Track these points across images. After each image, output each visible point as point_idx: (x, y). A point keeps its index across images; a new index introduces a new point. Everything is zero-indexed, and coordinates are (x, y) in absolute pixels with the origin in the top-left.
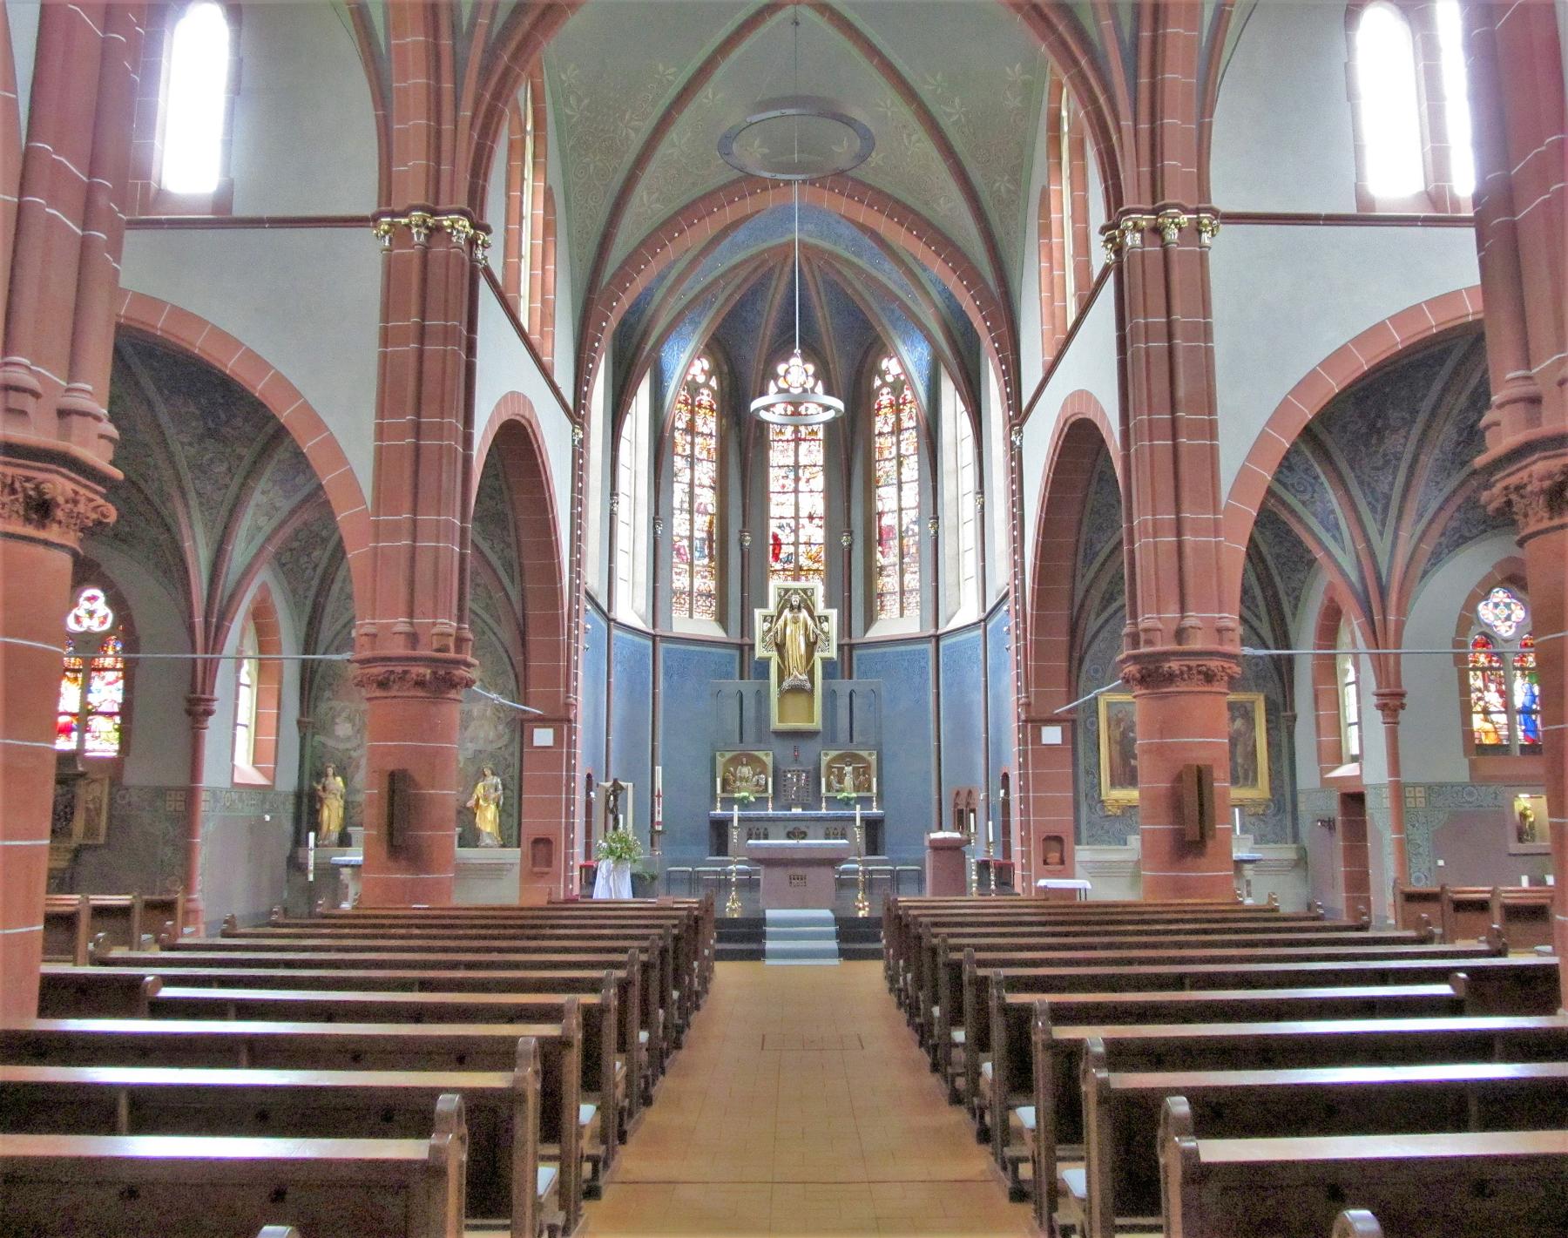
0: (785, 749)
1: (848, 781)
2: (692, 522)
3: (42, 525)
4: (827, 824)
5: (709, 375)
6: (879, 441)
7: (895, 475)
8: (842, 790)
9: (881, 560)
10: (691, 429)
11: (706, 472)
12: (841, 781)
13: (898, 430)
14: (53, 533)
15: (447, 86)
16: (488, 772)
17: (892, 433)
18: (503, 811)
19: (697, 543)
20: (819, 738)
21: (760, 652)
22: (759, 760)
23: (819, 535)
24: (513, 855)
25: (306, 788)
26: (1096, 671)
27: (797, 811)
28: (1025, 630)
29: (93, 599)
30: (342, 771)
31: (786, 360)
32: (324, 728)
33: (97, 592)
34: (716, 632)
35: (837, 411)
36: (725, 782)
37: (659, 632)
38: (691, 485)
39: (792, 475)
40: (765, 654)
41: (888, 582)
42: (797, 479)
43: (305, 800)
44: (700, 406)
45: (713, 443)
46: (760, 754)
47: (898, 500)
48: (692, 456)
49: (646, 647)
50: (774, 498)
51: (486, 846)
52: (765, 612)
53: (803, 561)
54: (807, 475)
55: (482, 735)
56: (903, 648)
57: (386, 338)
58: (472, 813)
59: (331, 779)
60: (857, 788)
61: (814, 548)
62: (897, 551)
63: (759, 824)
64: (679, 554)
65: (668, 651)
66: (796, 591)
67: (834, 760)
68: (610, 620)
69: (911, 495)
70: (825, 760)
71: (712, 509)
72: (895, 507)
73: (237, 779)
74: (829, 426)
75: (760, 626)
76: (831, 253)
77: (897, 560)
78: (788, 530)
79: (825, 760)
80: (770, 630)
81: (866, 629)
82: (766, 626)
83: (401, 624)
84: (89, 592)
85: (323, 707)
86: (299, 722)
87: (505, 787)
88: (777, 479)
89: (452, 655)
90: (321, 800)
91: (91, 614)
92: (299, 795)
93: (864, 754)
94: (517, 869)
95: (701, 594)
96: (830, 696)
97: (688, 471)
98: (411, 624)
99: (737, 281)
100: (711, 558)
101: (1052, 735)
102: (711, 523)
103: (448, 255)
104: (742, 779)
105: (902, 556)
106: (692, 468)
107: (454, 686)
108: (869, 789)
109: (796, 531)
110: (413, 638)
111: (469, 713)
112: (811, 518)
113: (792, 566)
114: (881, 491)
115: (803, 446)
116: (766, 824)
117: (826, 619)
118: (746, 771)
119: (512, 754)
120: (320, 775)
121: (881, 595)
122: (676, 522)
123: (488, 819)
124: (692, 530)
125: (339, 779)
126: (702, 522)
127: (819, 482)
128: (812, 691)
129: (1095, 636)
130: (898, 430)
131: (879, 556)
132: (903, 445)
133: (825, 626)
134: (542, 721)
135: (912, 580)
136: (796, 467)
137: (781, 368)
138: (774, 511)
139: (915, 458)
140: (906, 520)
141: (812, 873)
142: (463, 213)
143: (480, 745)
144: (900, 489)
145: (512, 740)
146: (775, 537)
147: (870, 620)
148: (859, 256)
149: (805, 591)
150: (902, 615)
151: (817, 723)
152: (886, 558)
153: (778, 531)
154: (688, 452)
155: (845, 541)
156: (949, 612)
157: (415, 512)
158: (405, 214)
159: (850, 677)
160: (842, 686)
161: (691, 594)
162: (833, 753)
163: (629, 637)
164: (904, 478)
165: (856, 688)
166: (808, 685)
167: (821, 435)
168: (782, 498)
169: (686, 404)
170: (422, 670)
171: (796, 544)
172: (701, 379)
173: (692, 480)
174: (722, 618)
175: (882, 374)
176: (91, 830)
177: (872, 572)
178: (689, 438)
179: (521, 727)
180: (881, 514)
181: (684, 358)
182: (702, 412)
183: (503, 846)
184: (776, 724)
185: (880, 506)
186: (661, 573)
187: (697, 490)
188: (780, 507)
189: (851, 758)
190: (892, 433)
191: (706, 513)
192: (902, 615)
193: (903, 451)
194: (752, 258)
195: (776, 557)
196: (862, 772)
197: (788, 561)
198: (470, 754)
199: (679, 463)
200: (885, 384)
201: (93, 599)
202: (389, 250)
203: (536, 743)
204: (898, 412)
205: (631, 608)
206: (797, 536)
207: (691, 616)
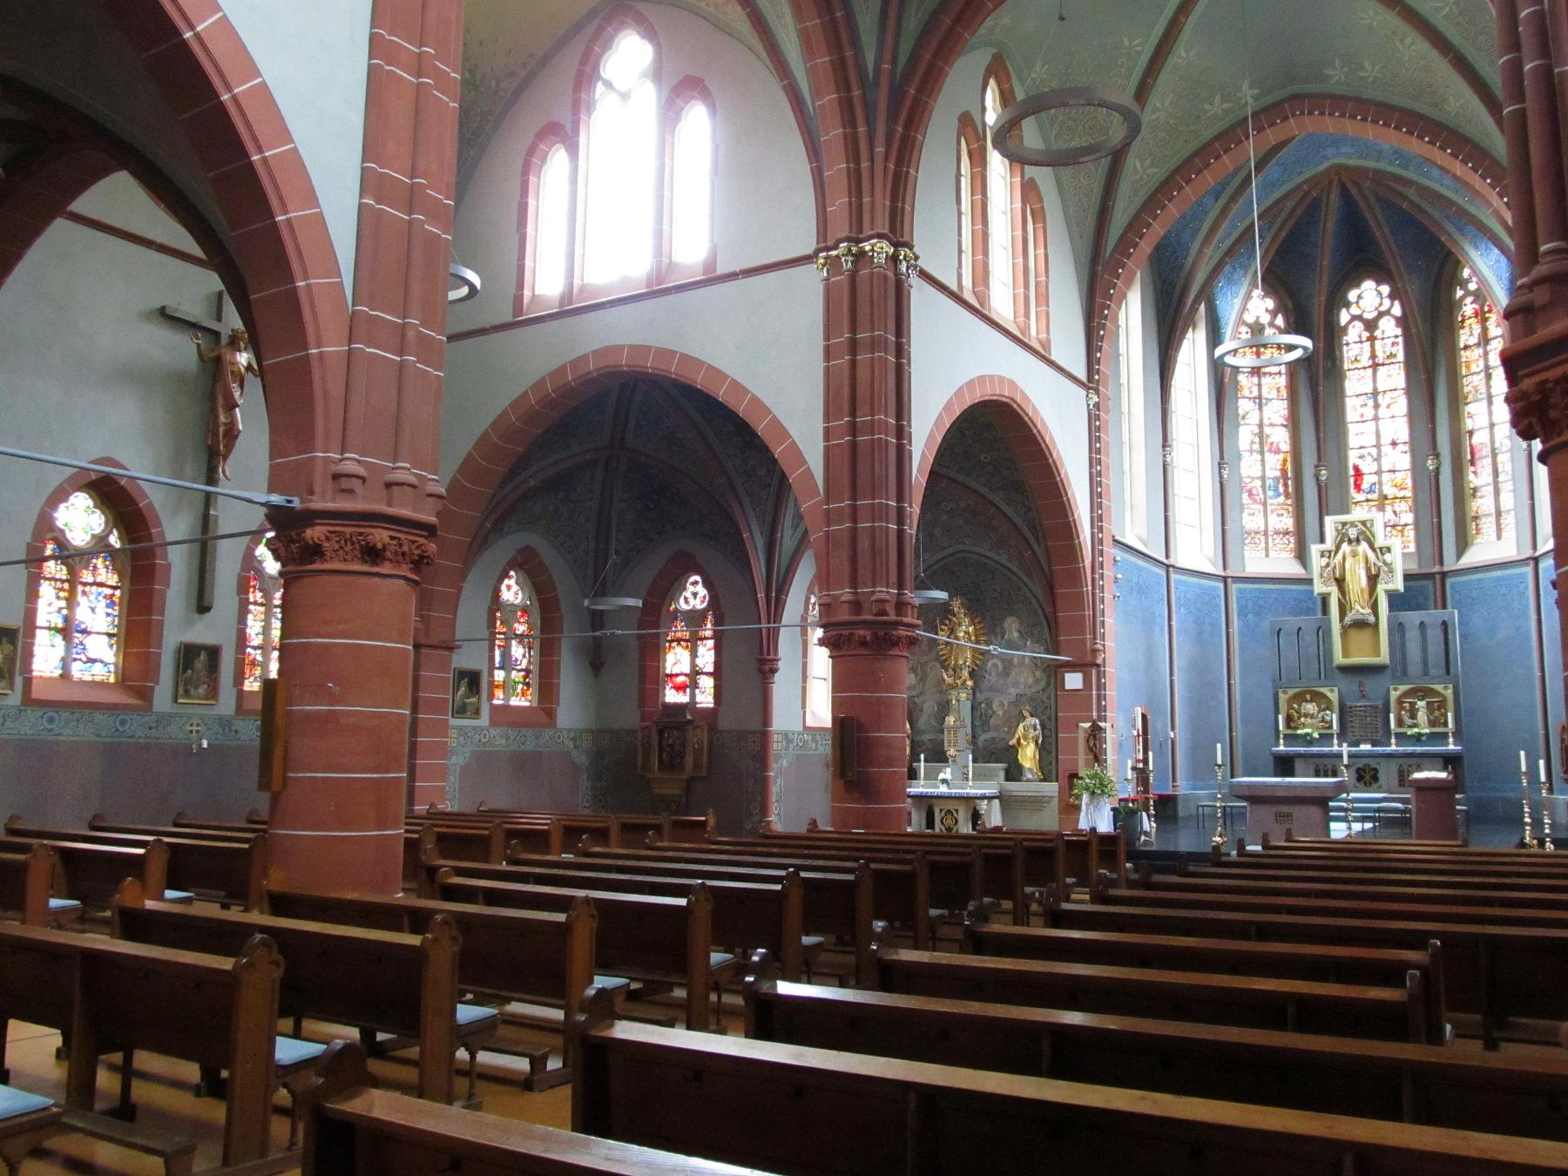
0: (1351, 684)
1: (1422, 716)
2: (1263, 461)
3: (375, 564)
4: (1401, 761)
5: (1274, 314)
7: (1483, 389)
8: (1415, 726)
9: (1473, 480)
11: (1278, 410)
12: (1413, 716)
14: (386, 569)
15: (861, 129)
16: (1026, 714)
17: (1478, 345)
18: (1042, 749)
19: (1268, 482)
20: (1389, 671)
21: (1319, 588)
22: (1323, 696)
24: (1051, 788)
29: (695, 583)
31: (1358, 286)
33: (698, 578)
35: (1305, 348)
36: (1289, 719)
37: (1229, 573)
38: (1261, 426)
39: (1371, 403)
40: (1324, 590)
41: (1483, 504)
42: (1377, 406)
45: (1282, 381)
48: (1260, 397)
50: (1353, 429)
53: (1389, 491)
56: (1499, 573)
57: (828, 354)
58: (1014, 750)
60: (1432, 723)
61: (1399, 477)
62: (1489, 469)
63: (1327, 761)
64: (1250, 494)
65: (1241, 591)
67: (1406, 694)
70: (1394, 695)
71: (1285, 447)
72: (1486, 424)
73: (809, 723)
74: (1292, 367)
75: (1317, 562)
76: (1376, 171)
77: (1490, 479)
78: (1369, 459)
79: (1394, 695)
82: (1324, 561)
83: (845, 594)
84: (692, 579)
87: (1043, 727)
88: (1354, 408)
89: (893, 617)
91: (695, 595)
93: (1439, 688)
94: (1055, 801)
95: (1277, 533)
96: (1397, 629)
98: (856, 594)
99: (1283, 216)
100: (1287, 496)
102: (1285, 461)
103: (872, 274)
104: (1306, 716)
105: (1496, 473)
106: (1260, 408)
107: (896, 643)
108: (1446, 724)
109: (1378, 459)
110: (856, 606)
113: (1375, 496)
114: (1470, 408)
115: (1381, 370)
117: (1389, 550)
118: (1310, 708)
121: (1476, 518)
123: (1028, 756)
124: (1263, 470)
127: (1401, 405)
128: (1376, 626)
130: (1485, 340)
131: (1471, 477)
133: (1388, 557)
136: (1375, 393)
138: (1353, 441)
142: (880, 236)
143: (1021, 689)
145: (1048, 684)
146: (1356, 468)
147: (1463, 545)
148: (1406, 168)
149: (1364, 523)
150: (1499, 537)
151: (1384, 657)
152: (1480, 477)
153: (1359, 462)
155: (1430, 464)
157: (854, 497)
158: (836, 247)
159: (1444, 607)
160: (1412, 618)
161: (1266, 534)
162: (1403, 688)
163: (1195, 580)
165: (1426, 620)
166: (1372, 619)
167: (1401, 357)
170: (861, 632)
171: (1379, 473)
172: (1265, 319)
173: (1261, 420)
176: (697, 766)
178: (1255, 380)
179: (1055, 673)
180: (1471, 433)
183: (1045, 780)
184: (1339, 658)
185: (1469, 424)
187: (1267, 430)
188: (1359, 436)
189: (1424, 693)
190: (1478, 345)
191: (1278, 451)
192: (1499, 537)
194: (1299, 187)
195: (1358, 487)
197: (1371, 491)
198: (1012, 698)
199: (1244, 406)
200: (1468, 293)
201: (695, 583)
202: (827, 279)
203: (1068, 687)
204: (1484, 321)
206: (1380, 465)
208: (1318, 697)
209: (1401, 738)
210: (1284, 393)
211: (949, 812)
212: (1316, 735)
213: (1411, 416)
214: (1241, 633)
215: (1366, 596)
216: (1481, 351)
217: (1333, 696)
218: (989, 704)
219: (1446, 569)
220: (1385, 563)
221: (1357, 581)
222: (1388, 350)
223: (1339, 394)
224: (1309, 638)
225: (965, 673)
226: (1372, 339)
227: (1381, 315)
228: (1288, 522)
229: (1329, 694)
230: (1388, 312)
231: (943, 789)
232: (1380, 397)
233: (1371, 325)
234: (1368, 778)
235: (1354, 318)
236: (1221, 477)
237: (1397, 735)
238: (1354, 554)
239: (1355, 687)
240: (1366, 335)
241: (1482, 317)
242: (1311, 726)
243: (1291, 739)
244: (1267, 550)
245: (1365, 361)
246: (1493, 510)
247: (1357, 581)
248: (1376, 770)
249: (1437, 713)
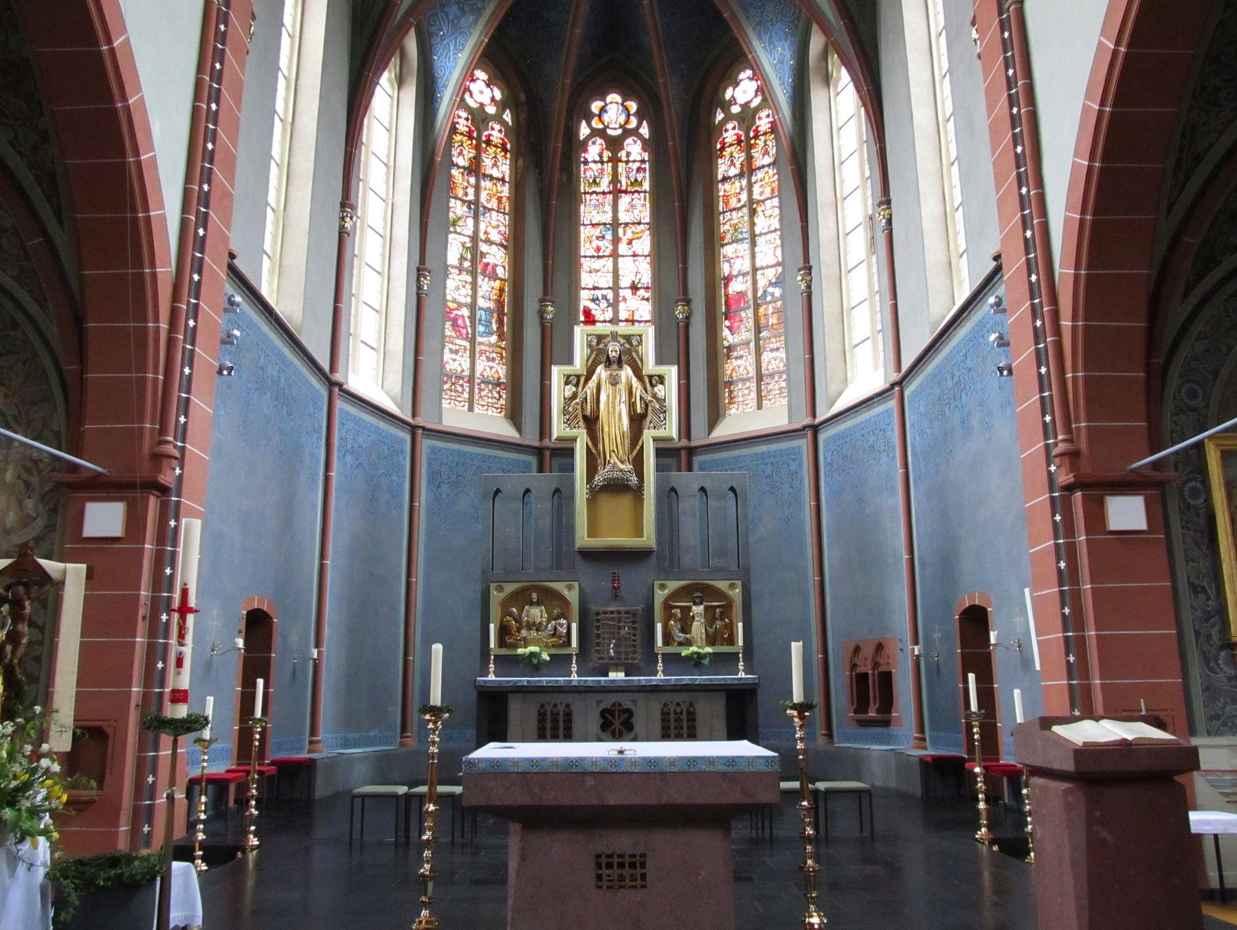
0: (598, 580)
1: (698, 628)
5: (502, 106)
6: (723, 189)
7: (745, 228)
8: (688, 643)
9: (728, 337)
10: (474, 168)
11: (496, 225)
12: (686, 629)
13: (748, 170)
19: (480, 314)
20: (653, 560)
21: (558, 428)
23: (644, 310)
26: (1192, 395)
27: (617, 676)
28: (1056, 315)
34: (506, 431)
36: (504, 631)
37: (420, 421)
38: (475, 238)
39: (609, 236)
40: (568, 432)
41: (740, 366)
42: (616, 241)
44: (488, 142)
45: (505, 191)
46: (559, 587)
47: (751, 255)
49: (403, 441)
50: (586, 264)
52: (568, 369)
54: (629, 235)
56: (763, 448)
60: (711, 640)
62: (751, 324)
63: (558, 699)
64: (455, 326)
65: (434, 450)
66: (614, 336)
67: (675, 595)
68: (334, 387)
69: (769, 252)
70: (660, 595)
72: (747, 266)
75: (558, 392)
77: (751, 336)
78: (604, 304)
79: (660, 595)
80: (574, 396)
81: (709, 433)
88: (589, 240)
93: (722, 585)
96: (668, 495)
97: (470, 221)
100: (501, 338)
101: (1126, 513)
102: (501, 290)
104: (530, 626)
105: (758, 329)
106: (476, 218)
108: (731, 641)
109: (614, 305)
112: (634, 288)
114: (728, 250)
115: (624, 200)
116: (568, 698)
117: (661, 379)
118: (536, 613)
121: (730, 383)
122: (450, 284)
126: (487, 287)
127: (644, 244)
128: (638, 492)
129: (1184, 329)
130: (748, 170)
131: (726, 332)
132: (756, 189)
133: (660, 390)
134: (103, 488)
135: (774, 360)
136: (615, 224)
137: (596, 106)
138: (586, 279)
139: (776, 202)
140: (762, 282)
141: (663, 847)
144: (753, 244)
146: (587, 312)
147: (715, 415)
149: (628, 338)
150: (760, 407)
151: (648, 537)
153: (591, 305)
154: (471, 197)
156: (833, 390)
161: (471, 379)
162: (673, 585)
164: (758, 230)
166: (634, 479)
167: (646, 186)
168: (597, 264)
169: (471, 138)
174: (514, 415)
175: (726, 106)
177: (716, 354)
178: (472, 180)
180: (728, 280)
181: (462, 58)
182: (491, 150)
184: (583, 538)
185: (726, 269)
186: (428, 344)
188: (593, 275)
191: (493, 276)
192: (760, 407)
193: (756, 196)
196: (720, 613)
199: (457, 208)
200: (729, 117)
205: (373, 373)
206: (616, 312)
207: (471, 409)
208: (549, 598)
209: (673, 661)
210: (506, 205)
212: (545, 657)
213: (657, 257)
214: (431, 513)
215: (627, 442)
216: (744, 182)
217: (573, 596)
219: (693, 444)
220: (654, 396)
221: (615, 422)
222: (633, 175)
223: (572, 221)
224: (542, 506)
226: (615, 160)
227: (627, 133)
228: (500, 370)
229: (566, 593)
230: (635, 132)
232: (621, 231)
233: (615, 144)
234: (617, 724)
235: (595, 133)
236: (419, 288)
237: (668, 658)
238: (614, 382)
239: (606, 584)
240: (606, 154)
241: (746, 144)
242: (535, 642)
243: (508, 663)
244: (471, 402)
245: (605, 185)
246: (752, 373)
247: (615, 422)
248: (630, 713)
249: (719, 623)
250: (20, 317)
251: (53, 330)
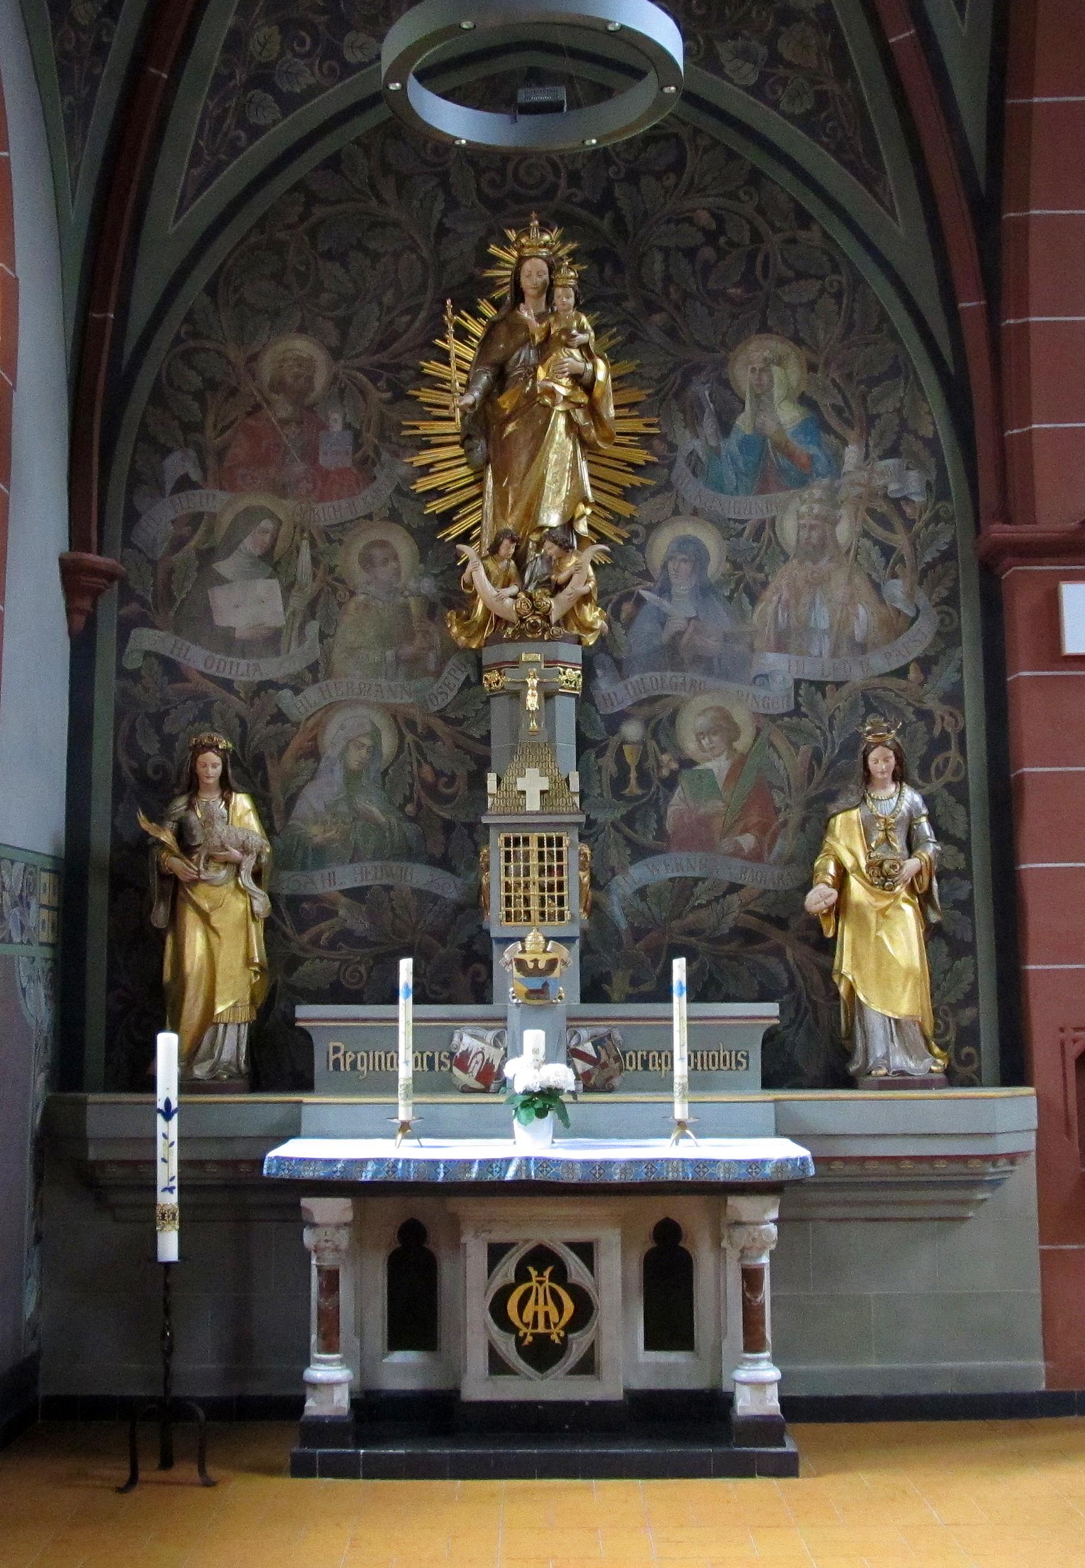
16: (881, 762)
24: (1009, 1115)
25: (101, 839)
30: (247, 772)
32: (176, 596)
43: (98, 895)
51: (902, 1081)
55: (822, 619)
59: (211, 799)
85: (160, 520)
86: (73, 577)
90: (176, 891)
92: (71, 868)
94: (1026, 1175)
111: (764, 530)
119: (954, 698)
120: (165, 783)
123: (888, 962)
125: (242, 802)
143: (816, 664)
145: (948, 637)
183: (952, 1078)
198: (778, 696)
211: (542, 1257)
218: (662, 727)
225: (580, 570)
231: (529, 1144)
250: (813, 205)
251: (902, 233)
